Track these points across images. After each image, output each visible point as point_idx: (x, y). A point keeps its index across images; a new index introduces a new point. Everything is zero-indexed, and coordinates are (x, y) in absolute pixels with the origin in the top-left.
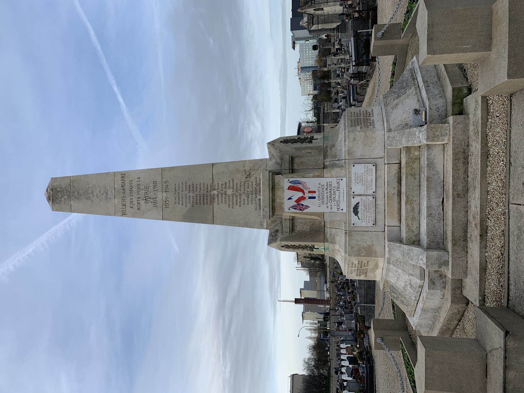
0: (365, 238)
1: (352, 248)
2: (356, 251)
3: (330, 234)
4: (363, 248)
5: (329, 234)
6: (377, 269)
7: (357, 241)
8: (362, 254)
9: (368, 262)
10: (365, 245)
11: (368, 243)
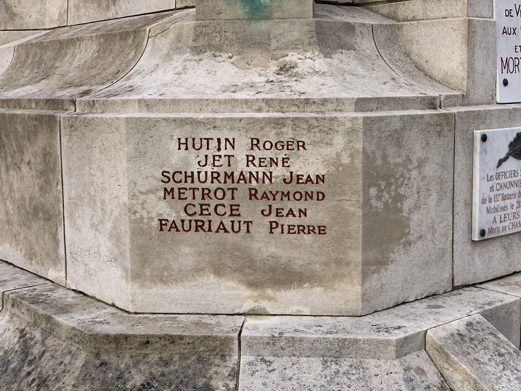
0: (432, 201)
1: (397, 138)
2: (385, 157)
3: (350, 28)
4: (399, 198)
5: (352, 21)
6: (252, 285)
7: (421, 163)
8: (373, 191)
9: (322, 230)
10: (407, 204)
11: (415, 217)
